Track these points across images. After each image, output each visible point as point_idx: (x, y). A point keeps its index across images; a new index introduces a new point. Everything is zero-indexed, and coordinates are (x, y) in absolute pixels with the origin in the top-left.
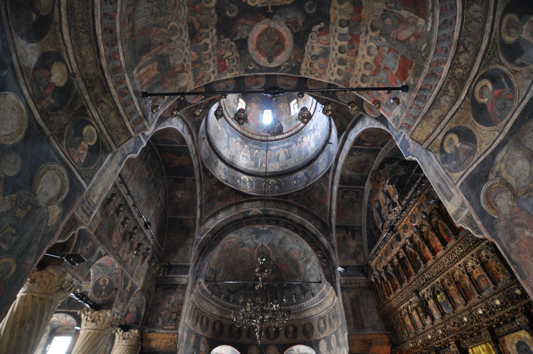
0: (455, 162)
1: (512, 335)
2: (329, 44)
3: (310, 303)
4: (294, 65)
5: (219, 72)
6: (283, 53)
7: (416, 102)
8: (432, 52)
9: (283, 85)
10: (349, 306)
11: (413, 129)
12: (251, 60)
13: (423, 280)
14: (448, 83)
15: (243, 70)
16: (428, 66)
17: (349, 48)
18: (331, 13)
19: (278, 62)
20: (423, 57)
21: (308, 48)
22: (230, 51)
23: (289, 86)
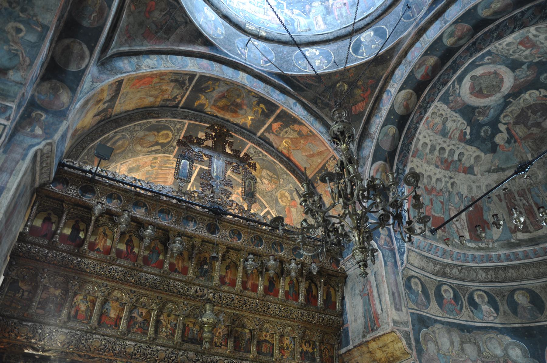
2: (450, 138)
4: (451, 98)
6: (468, 91)
7: (428, 245)
9: (424, 61)
11: (413, 249)
12: (494, 62)
13: (196, 291)
15: (495, 51)
18: (474, 148)
19: (465, 84)
21: (456, 117)
23: (419, 68)
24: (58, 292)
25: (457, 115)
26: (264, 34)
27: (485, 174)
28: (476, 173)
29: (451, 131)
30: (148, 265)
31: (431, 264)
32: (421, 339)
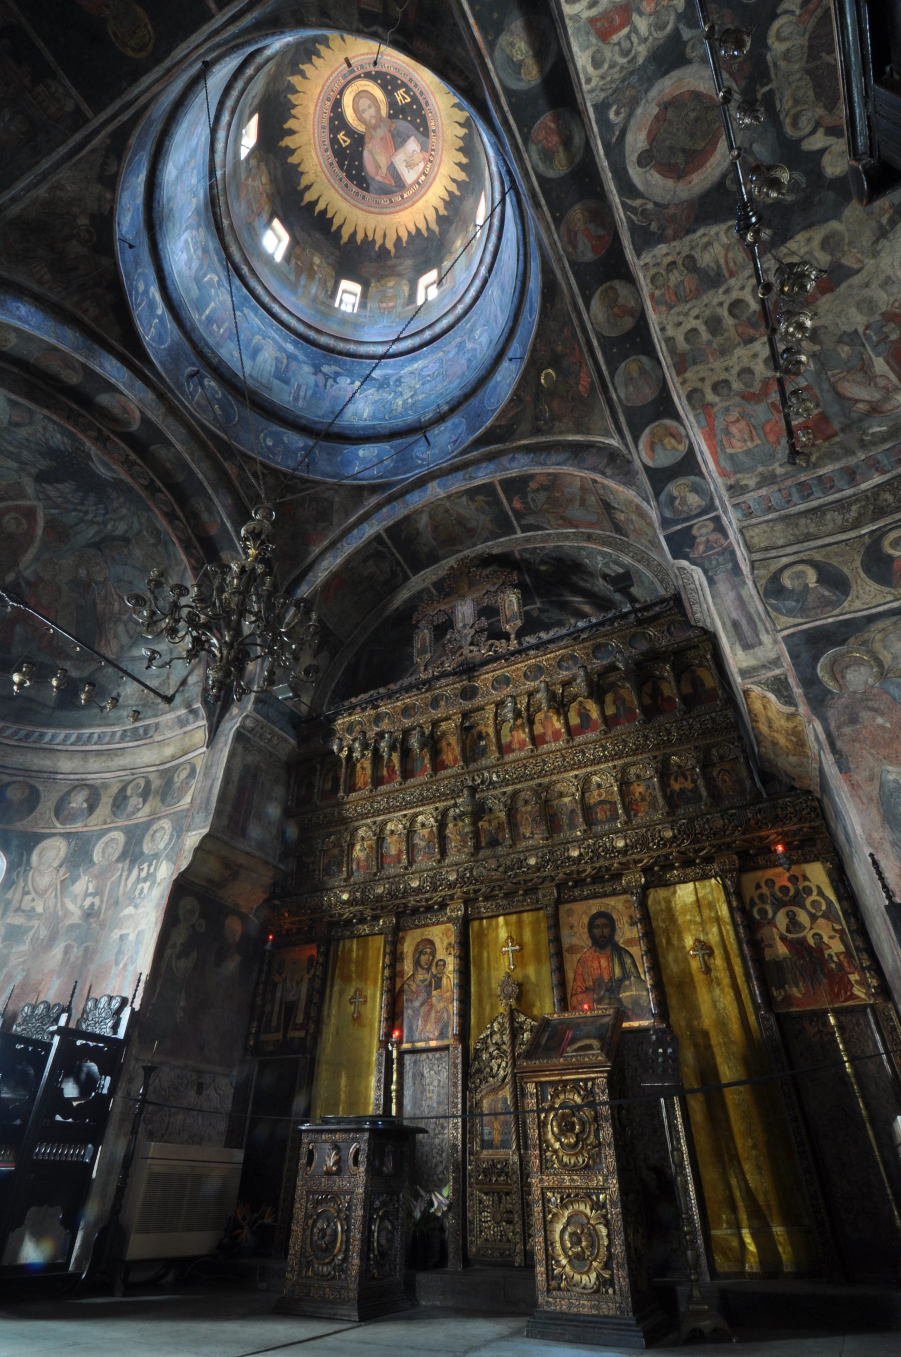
0: (794, 603)
1: (591, 902)
2: (732, 274)
3: (73, 739)
4: (654, 227)
5: (592, 21)
6: (670, 183)
7: (794, 490)
8: (887, 446)
9: (569, 231)
10: (235, 777)
11: (754, 521)
12: (634, 103)
13: (474, 780)
14: (857, 500)
15: (603, 95)
16: (863, 457)
17: (748, 319)
19: (647, 183)
20: (862, 440)
21: (704, 235)
22: (650, 26)
23: (575, 247)
24: (336, 851)
25: (701, 232)
26: (446, 408)
27: (879, 247)
28: (856, 266)
29: (722, 262)
30: (413, 776)
31: (828, 516)
32: (820, 672)
